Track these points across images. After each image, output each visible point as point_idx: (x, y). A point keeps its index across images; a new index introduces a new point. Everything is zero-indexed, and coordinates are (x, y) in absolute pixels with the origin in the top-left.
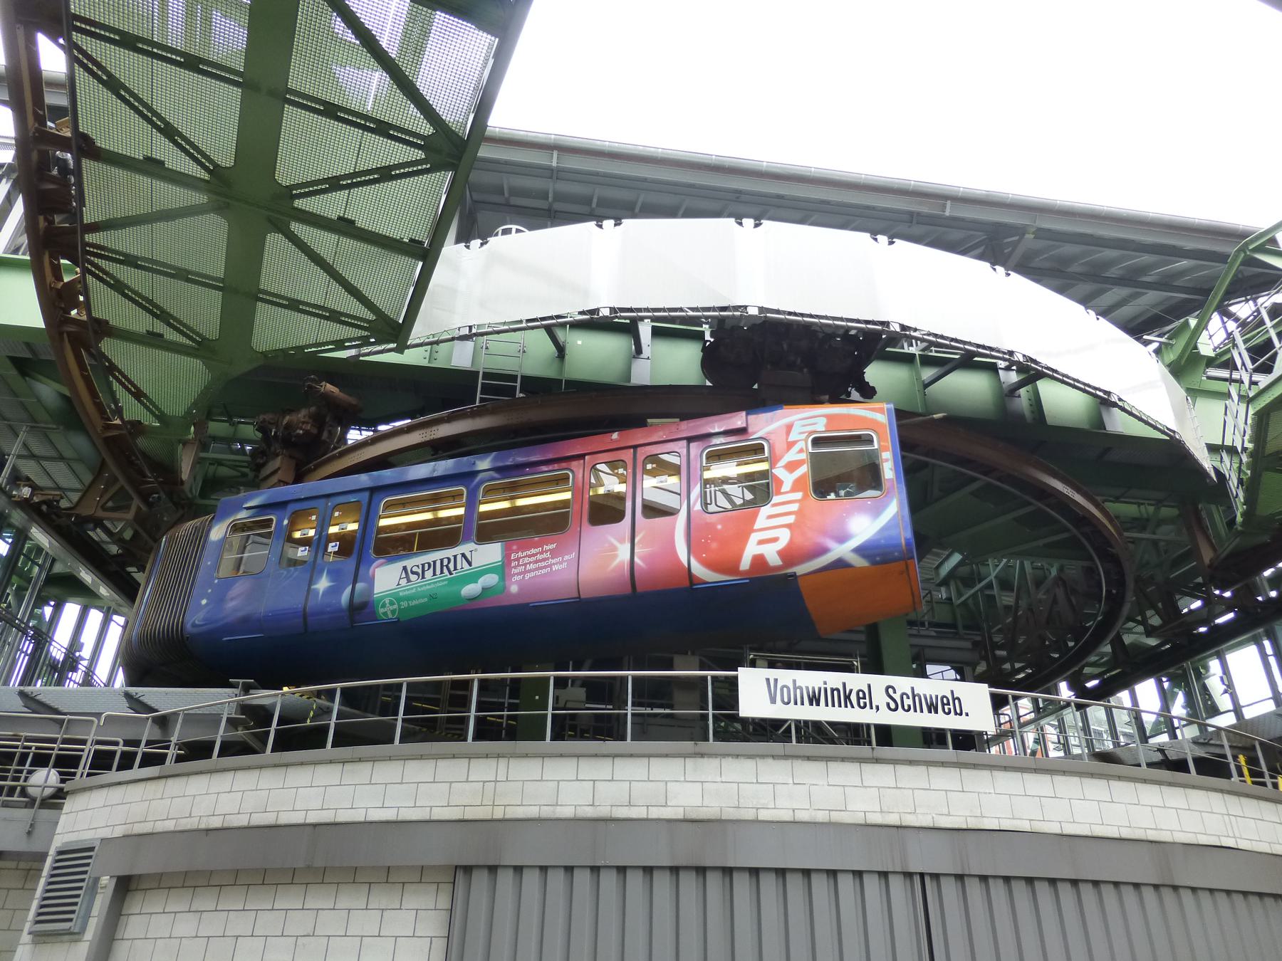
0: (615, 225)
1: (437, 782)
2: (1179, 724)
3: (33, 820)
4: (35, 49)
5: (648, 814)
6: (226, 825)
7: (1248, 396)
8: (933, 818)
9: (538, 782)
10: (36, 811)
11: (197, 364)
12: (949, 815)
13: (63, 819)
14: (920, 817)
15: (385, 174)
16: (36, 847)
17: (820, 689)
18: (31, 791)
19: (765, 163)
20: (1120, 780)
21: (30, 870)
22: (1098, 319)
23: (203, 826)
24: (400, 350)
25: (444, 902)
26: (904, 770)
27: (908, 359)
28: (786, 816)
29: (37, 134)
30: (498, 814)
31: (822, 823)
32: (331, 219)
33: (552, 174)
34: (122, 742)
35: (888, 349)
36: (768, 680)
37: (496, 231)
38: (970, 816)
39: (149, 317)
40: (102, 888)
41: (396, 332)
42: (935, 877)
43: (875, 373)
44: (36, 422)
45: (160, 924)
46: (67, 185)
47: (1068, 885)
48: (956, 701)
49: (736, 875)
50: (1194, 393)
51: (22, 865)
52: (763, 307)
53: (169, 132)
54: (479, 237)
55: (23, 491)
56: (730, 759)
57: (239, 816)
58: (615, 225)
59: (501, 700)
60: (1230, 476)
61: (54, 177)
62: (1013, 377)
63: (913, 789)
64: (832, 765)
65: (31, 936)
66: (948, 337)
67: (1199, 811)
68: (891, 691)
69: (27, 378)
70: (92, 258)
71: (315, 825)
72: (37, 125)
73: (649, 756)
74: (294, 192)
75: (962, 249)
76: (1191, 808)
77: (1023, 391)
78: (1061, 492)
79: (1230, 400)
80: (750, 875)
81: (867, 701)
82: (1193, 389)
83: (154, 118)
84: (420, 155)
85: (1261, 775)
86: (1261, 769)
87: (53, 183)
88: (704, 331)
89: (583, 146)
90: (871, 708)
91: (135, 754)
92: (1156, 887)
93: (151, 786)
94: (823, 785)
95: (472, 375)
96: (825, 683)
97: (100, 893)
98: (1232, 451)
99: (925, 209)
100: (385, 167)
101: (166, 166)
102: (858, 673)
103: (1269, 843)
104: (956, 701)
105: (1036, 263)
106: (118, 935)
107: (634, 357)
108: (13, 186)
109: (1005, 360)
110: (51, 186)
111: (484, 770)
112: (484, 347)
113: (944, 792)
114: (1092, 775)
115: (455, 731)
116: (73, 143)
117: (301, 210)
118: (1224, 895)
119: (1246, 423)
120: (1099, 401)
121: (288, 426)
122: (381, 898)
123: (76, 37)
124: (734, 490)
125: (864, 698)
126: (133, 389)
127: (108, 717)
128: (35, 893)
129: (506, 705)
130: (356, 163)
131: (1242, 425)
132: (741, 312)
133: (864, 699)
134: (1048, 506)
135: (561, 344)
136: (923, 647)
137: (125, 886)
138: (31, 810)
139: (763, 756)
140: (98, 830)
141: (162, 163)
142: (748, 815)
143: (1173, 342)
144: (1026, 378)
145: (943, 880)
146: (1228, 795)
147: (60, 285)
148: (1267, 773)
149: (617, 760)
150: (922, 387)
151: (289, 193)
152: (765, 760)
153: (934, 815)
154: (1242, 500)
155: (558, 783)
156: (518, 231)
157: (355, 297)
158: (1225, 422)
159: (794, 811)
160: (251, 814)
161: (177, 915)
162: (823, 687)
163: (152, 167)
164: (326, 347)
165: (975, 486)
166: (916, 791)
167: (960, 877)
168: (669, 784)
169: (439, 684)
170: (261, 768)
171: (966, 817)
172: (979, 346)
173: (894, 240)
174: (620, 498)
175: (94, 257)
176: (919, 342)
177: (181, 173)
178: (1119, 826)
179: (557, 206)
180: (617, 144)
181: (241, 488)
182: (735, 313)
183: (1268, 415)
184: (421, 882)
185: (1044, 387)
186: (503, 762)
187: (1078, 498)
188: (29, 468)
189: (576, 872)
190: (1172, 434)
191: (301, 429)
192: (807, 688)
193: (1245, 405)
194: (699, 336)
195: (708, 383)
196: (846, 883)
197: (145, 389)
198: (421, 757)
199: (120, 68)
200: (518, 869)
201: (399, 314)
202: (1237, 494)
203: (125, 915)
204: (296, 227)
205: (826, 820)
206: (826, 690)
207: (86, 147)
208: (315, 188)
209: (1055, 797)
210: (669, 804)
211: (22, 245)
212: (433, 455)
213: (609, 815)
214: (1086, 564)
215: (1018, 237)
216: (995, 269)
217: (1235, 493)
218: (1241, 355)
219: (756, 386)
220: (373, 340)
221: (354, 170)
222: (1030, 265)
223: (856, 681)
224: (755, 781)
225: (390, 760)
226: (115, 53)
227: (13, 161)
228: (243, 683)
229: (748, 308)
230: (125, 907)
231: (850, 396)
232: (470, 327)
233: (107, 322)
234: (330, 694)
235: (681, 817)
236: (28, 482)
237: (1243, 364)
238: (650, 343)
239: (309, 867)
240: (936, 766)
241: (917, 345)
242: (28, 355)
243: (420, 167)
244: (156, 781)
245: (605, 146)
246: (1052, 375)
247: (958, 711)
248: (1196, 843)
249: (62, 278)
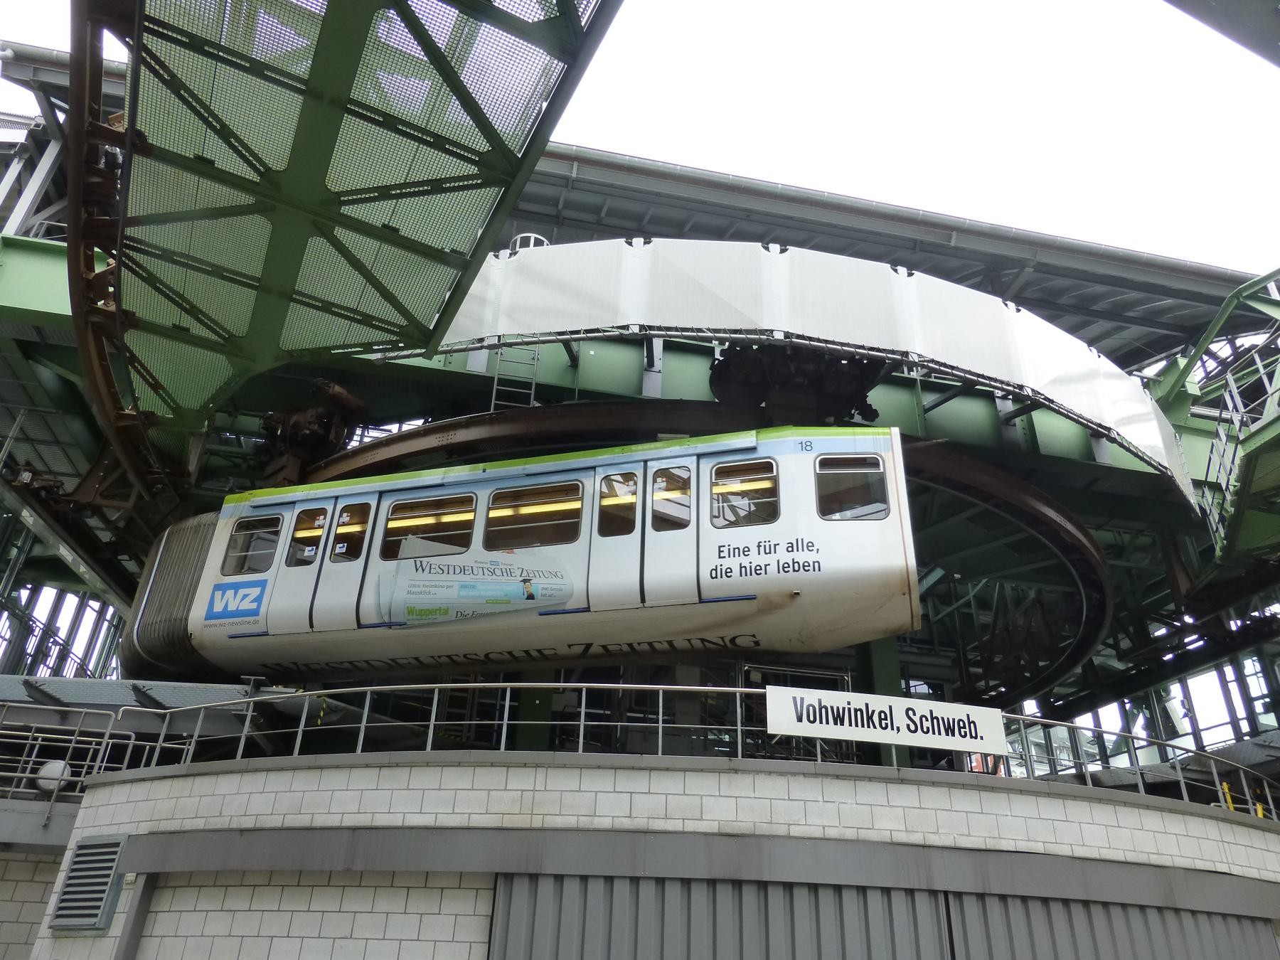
0: (645, 243)
1: (475, 790)
2: (1174, 753)
3: (49, 813)
5: (683, 828)
6: (258, 825)
7: (1238, 438)
8: (954, 838)
9: (576, 793)
11: (222, 358)
12: (969, 835)
13: (81, 813)
14: (943, 837)
15: (437, 187)
16: (51, 839)
17: (844, 709)
18: (41, 782)
20: (1125, 806)
21: (39, 862)
22: (1099, 357)
23: (234, 826)
24: (428, 356)
25: (484, 908)
26: (928, 791)
27: (909, 384)
28: (817, 833)
29: (90, 128)
30: (537, 823)
32: (376, 226)
33: (567, 182)
34: (133, 736)
35: (893, 374)
36: (794, 699)
37: (515, 238)
39: (177, 310)
41: (427, 338)
42: (959, 895)
43: (878, 397)
44: (35, 405)
45: (190, 923)
47: (1137, 911)
48: (972, 725)
49: (771, 890)
50: (1180, 429)
51: (32, 857)
52: (788, 332)
53: (225, 133)
54: (506, 247)
55: (24, 476)
56: (763, 775)
58: (645, 243)
59: (494, 702)
60: (1210, 510)
61: (100, 170)
62: (1008, 406)
65: (51, 930)
67: (1197, 838)
68: (911, 713)
69: (30, 361)
70: (128, 251)
71: (354, 829)
72: (90, 119)
73: (685, 770)
74: (342, 198)
75: (958, 277)
77: (1018, 420)
79: (1218, 440)
80: (784, 889)
81: (889, 721)
82: (1179, 426)
83: (206, 115)
84: (474, 170)
85: (1245, 802)
86: (1245, 795)
87: (99, 176)
88: (714, 348)
89: (604, 159)
90: (893, 729)
91: (127, 746)
92: (1160, 909)
94: (852, 804)
95: (487, 381)
96: (849, 703)
97: (126, 889)
98: (1216, 487)
100: (436, 180)
102: (848, 691)
103: (1258, 869)
104: (972, 725)
105: (1029, 294)
107: (646, 370)
108: (24, 167)
109: (1002, 390)
110: (97, 180)
113: (965, 814)
114: (1191, 814)
115: (485, 739)
117: (346, 216)
118: (1205, 917)
119: (1233, 462)
121: (296, 425)
122: (422, 902)
123: (147, 39)
124: (737, 502)
125: (886, 719)
126: (150, 380)
128: (53, 887)
129: (498, 708)
130: (408, 173)
131: (1228, 465)
133: (886, 720)
135: (575, 353)
137: (154, 884)
139: (794, 774)
140: (121, 825)
141: (212, 162)
142: (781, 831)
143: (1161, 379)
144: (1021, 408)
145: (965, 898)
146: (1222, 823)
148: (1250, 800)
149: (654, 774)
151: (337, 199)
152: (797, 778)
153: (956, 836)
154: (1223, 535)
156: (538, 243)
158: (1210, 458)
159: (824, 828)
160: (285, 815)
161: (209, 913)
162: (847, 706)
163: (202, 166)
164: (353, 350)
166: (938, 811)
167: (981, 896)
171: (985, 837)
172: (979, 376)
173: (913, 272)
174: (630, 508)
175: (129, 250)
176: (919, 368)
177: (242, 177)
179: (566, 213)
180: (637, 159)
181: (230, 478)
183: (1257, 457)
184: (459, 888)
185: (1039, 417)
187: (1069, 527)
189: (667, 884)
191: (308, 429)
192: (832, 708)
194: (709, 352)
195: (717, 400)
196: (875, 900)
197: (163, 380)
198: (459, 765)
200: (559, 878)
202: (1217, 528)
204: (340, 233)
205: (854, 837)
206: (849, 709)
207: (137, 143)
208: (359, 196)
210: (704, 818)
211: (34, 226)
212: (447, 459)
213: (646, 828)
214: (1067, 589)
216: (1006, 305)
218: (1233, 395)
219: (763, 405)
220: (400, 345)
221: (405, 181)
222: (1023, 296)
223: (878, 702)
224: (787, 798)
225: (428, 766)
228: (254, 679)
230: (153, 904)
231: (853, 418)
232: (499, 337)
233: (134, 314)
236: (29, 466)
237: (1235, 407)
238: (661, 358)
239: (348, 870)
241: (917, 371)
242: (36, 339)
243: (466, 183)
244: (184, 778)
246: (1046, 404)
247: (974, 735)
248: (1193, 868)
249: (94, 268)
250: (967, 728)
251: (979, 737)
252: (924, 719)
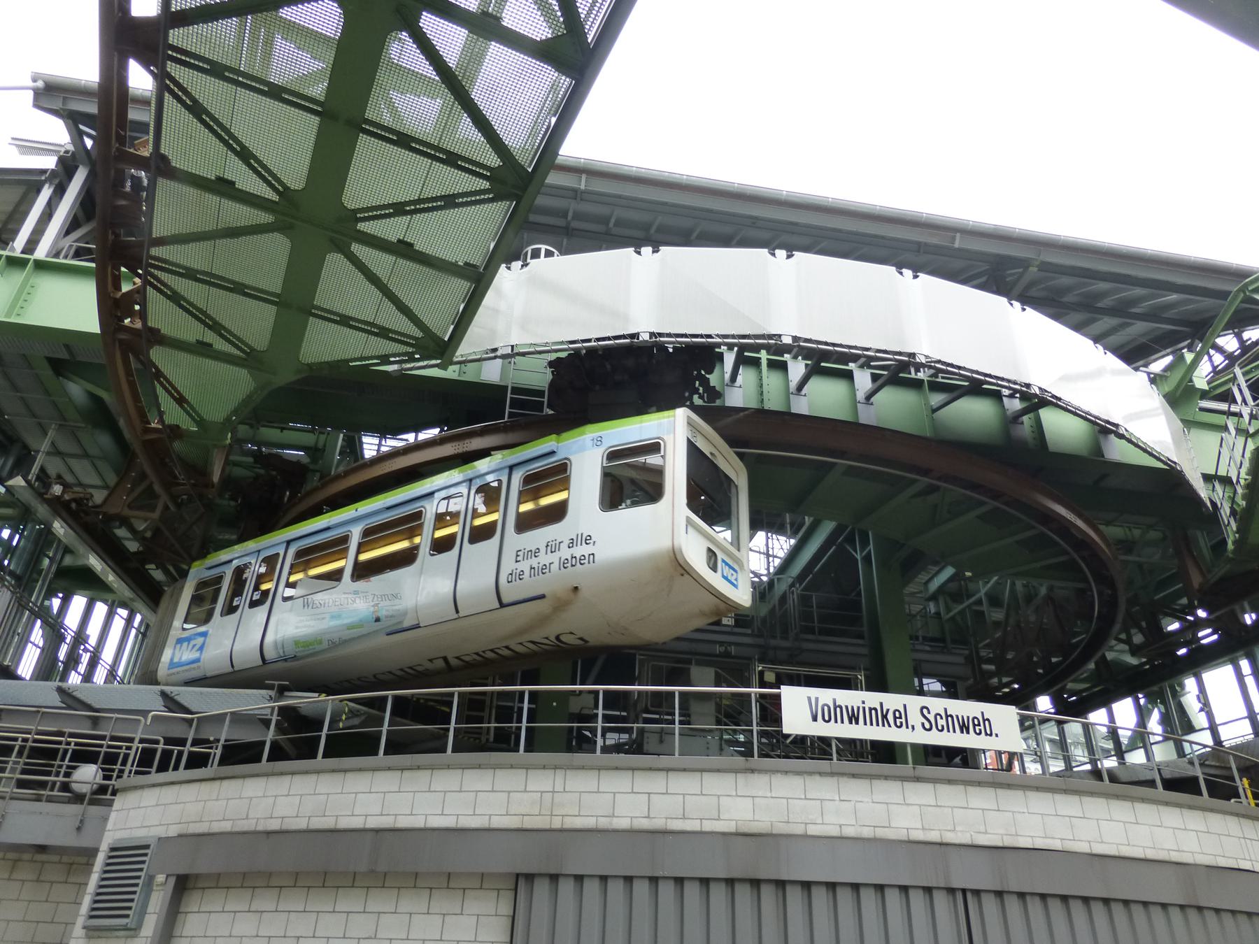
0: (653, 252)
1: (495, 791)
4: (125, 75)
6: (285, 827)
8: (971, 836)
10: (85, 808)
11: (243, 373)
12: (986, 833)
13: (113, 816)
14: (959, 834)
15: (450, 201)
16: (84, 842)
17: (858, 708)
18: (75, 786)
19: (784, 192)
20: (1143, 802)
22: (1106, 353)
23: (260, 828)
24: (443, 367)
25: (505, 908)
26: (944, 789)
27: (916, 385)
28: (834, 831)
29: (117, 154)
30: (557, 823)
31: (868, 840)
33: (575, 194)
34: (162, 740)
35: (901, 375)
36: (809, 699)
37: (524, 251)
38: (1006, 835)
39: (200, 326)
40: (157, 885)
41: (442, 349)
42: (977, 893)
46: (138, 202)
47: (1159, 909)
48: (987, 722)
49: (789, 888)
50: (1189, 424)
51: (65, 859)
53: (245, 155)
54: (517, 259)
55: (55, 488)
56: (779, 775)
57: (298, 819)
58: (653, 252)
59: (510, 704)
60: (1222, 504)
61: (126, 193)
62: (1015, 405)
63: (952, 808)
64: (876, 783)
66: (945, 363)
67: (1218, 834)
68: (925, 711)
69: (61, 378)
70: (153, 270)
71: (377, 831)
72: (117, 145)
73: (702, 771)
74: (358, 215)
76: (1210, 831)
77: (1025, 418)
78: (1065, 517)
81: (903, 720)
83: (227, 138)
84: (485, 185)
88: (722, 353)
90: (907, 727)
91: (155, 750)
92: (1182, 907)
93: (205, 787)
94: (868, 802)
96: (863, 702)
97: (157, 890)
98: (1226, 481)
99: (934, 241)
100: (449, 195)
101: (237, 186)
102: (862, 690)
104: (987, 722)
105: (1033, 292)
106: (177, 932)
108: (54, 191)
109: (1009, 388)
110: (123, 202)
111: (541, 782)
112: (513, 363)
114: (1212, 810)
115: (504, 742)
116: (153, 164)
119: (1243, 456)
120: (1097, 428)
122: (443, 902)
123: (171, 68)
125: (900, 718)
126: (175, 394)
127: (154, 717)
129: (516, 710)
131: (1238, 459)
132: (775, 340)
133: (900, 718)
134: (1049, 530)
136: (921, 661)
137: (183, 885)
138: (80, 806)
139: (811, 773)
141: (233, 183)
142: (799, 830)
143: (1168, 374)
145: (983, 895)
147: (119, 295)
149: (670, 773)
150: (930, 412)
151: (354, 216)
152: (813, 777)
153: (972, 833)
154: (1235, 529)
155: (614, 795)
156: (549, 254)
157: (407, 316)
159: (840, 826)
163: (223, 187)
164: (371, 362)
165: (983, 510)
166: (955, 809)
167: (999, 894)
168: (721, 798)
169: (484, 693)
170: (318, 773)
171: (1002, 835)
175: (154, 269)
178: (1117, 844)
179: (575, 224)
180: (643, 170)
182: (770, 341)
185: (1047, 415)
186: (560, 773)
187: (1080, 523)
188: (55, 465)
190: (1173, 465)
192: (847, 707)
193: (1243, 439)
196: (893, 897)
198: (479, 767)
199: (204, 94)
200: (579, 879)
201: (445, 333)
203: (183, 913)
204: (357, 248)
206: (864, 708)
207: (161, 166)
209: (1084, 818)
213: (665, 827)
214: (1081, 585)
215: (1021, 270)
216: (1011, 304)
217: (1226, 522)
220: (417, 356)
221: (419, 197)
222: (1028, 295)
223: (892, 701)
224: (803, 797)
225: (449, 768)
226: (201, 80)
227: (56, 167)
229: (783, 338)
230: (183, 903)
232: (512, 346)
233: (159, 331)
234: (379, 703)
235: (733, 830)
237: (1244, 401)
239: (372, 871)
240: (973, 786)
241: (924, 372)
243: (478, 198)
245: (632, 171)
246: (1054, 402)
247: (989, 732)
250: (982, 726)
251: (994, 735)
252: (938, 717)
